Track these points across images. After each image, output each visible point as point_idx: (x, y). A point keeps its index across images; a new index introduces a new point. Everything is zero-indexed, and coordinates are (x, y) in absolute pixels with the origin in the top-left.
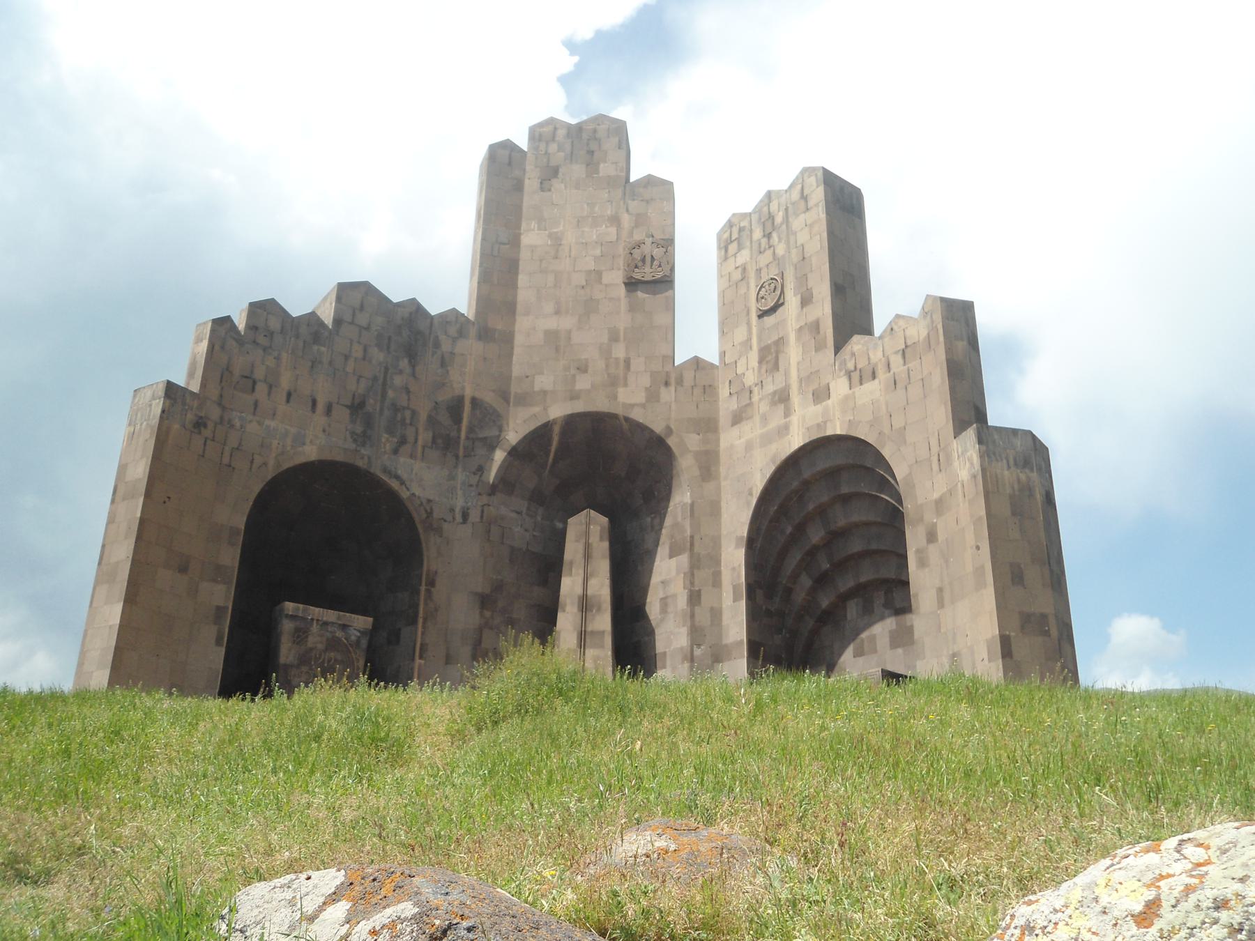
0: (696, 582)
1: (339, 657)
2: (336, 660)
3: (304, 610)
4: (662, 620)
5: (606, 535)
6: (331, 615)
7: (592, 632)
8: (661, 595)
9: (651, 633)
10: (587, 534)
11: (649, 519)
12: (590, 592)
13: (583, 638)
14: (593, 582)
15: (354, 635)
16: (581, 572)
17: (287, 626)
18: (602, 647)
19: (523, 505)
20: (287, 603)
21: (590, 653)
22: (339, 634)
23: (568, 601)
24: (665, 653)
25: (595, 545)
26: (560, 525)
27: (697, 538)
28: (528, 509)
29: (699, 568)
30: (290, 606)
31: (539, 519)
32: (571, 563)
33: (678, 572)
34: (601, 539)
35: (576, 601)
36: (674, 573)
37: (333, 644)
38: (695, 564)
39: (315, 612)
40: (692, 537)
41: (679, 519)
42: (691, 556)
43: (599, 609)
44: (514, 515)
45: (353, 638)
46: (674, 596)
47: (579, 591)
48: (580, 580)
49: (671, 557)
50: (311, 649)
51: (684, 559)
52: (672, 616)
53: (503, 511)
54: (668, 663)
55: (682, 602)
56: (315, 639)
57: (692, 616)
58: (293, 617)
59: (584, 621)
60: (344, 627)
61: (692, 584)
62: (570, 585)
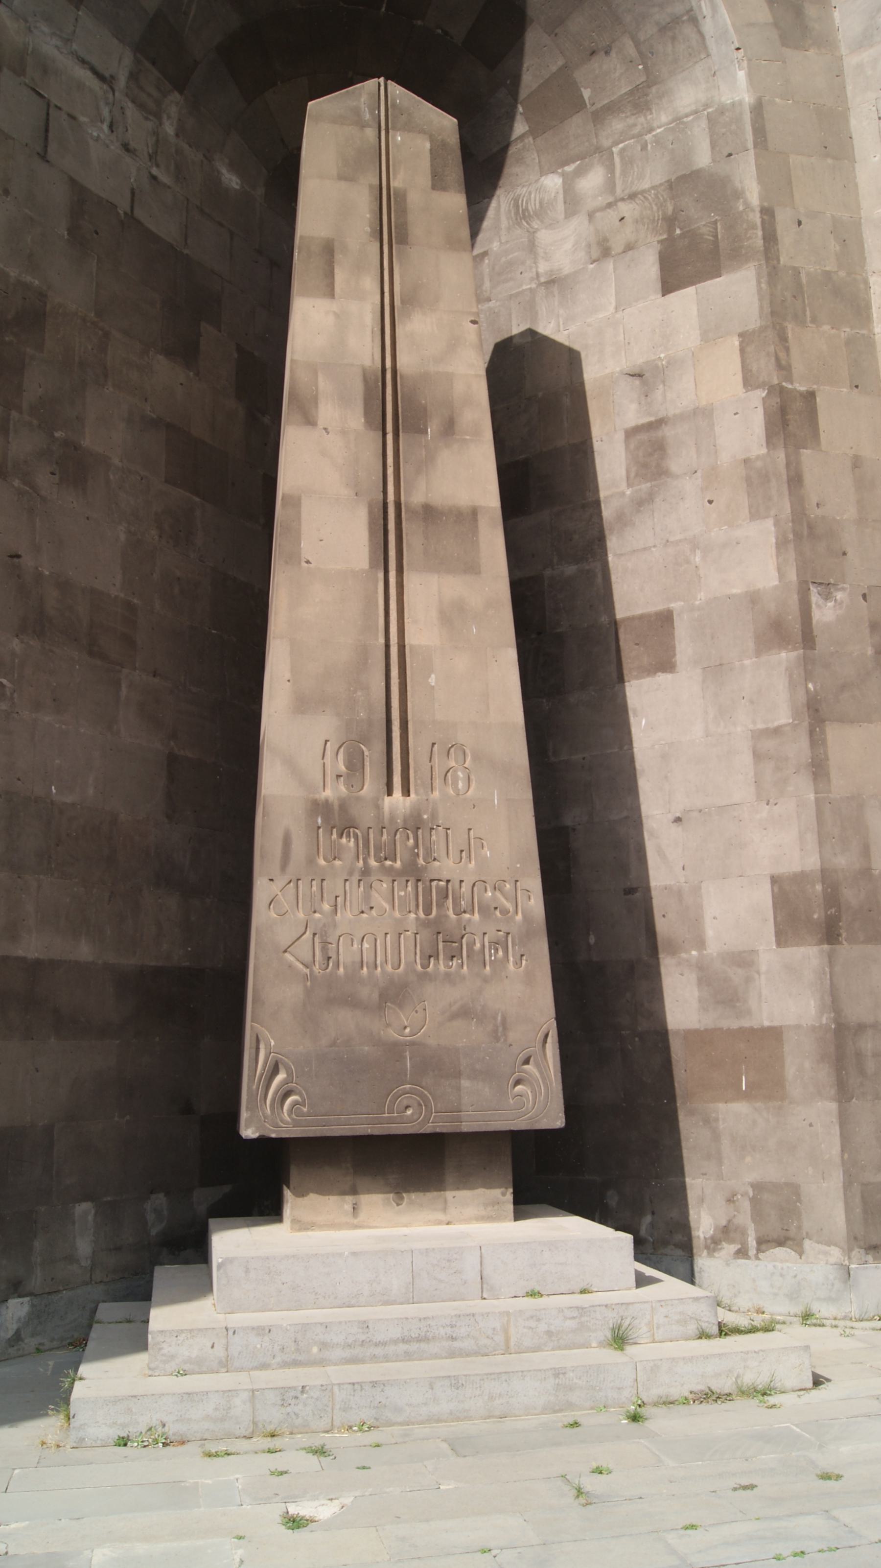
0: (798, 367)
4: (642, 503)
5: (455, 172)
7: (430, 514)
8: (632, 414)
9: (592, 546)
10: (381, 158)
11: (553, 182)
12: (406, 361)
13: (392, 530)
14: (420, 333)
16: (370, 284)
18: (472, 568)
19: (121, 62)
21: (424, 591)
23: (324, 384)
24: (666, 619)
25: (414, 199)
26: (232, 180)
27: (783, 218)
28: (133, 77)
29: (800, 320)
31: (169, 129)
32: (329, 251)
33: (710, 334)
34: (438, 182)
35: (358, 388)
36: (688, 337)
38: (786, 306)
40: (768, 213)
41: (703, 158)
42: (772, 269)
43: (449, 428)
44: (84, 75)
46: (702, 415)
47: (364, 350)
48: (365, 313)
49: (667, 288)
51: (738, 290)
52: (690, 486)
53: (47, 44)
54: (685, 646)
55: (742, 430)
57: (795, 481)
59: (391, 470)
61: (784, 368)
62: (326, 330)
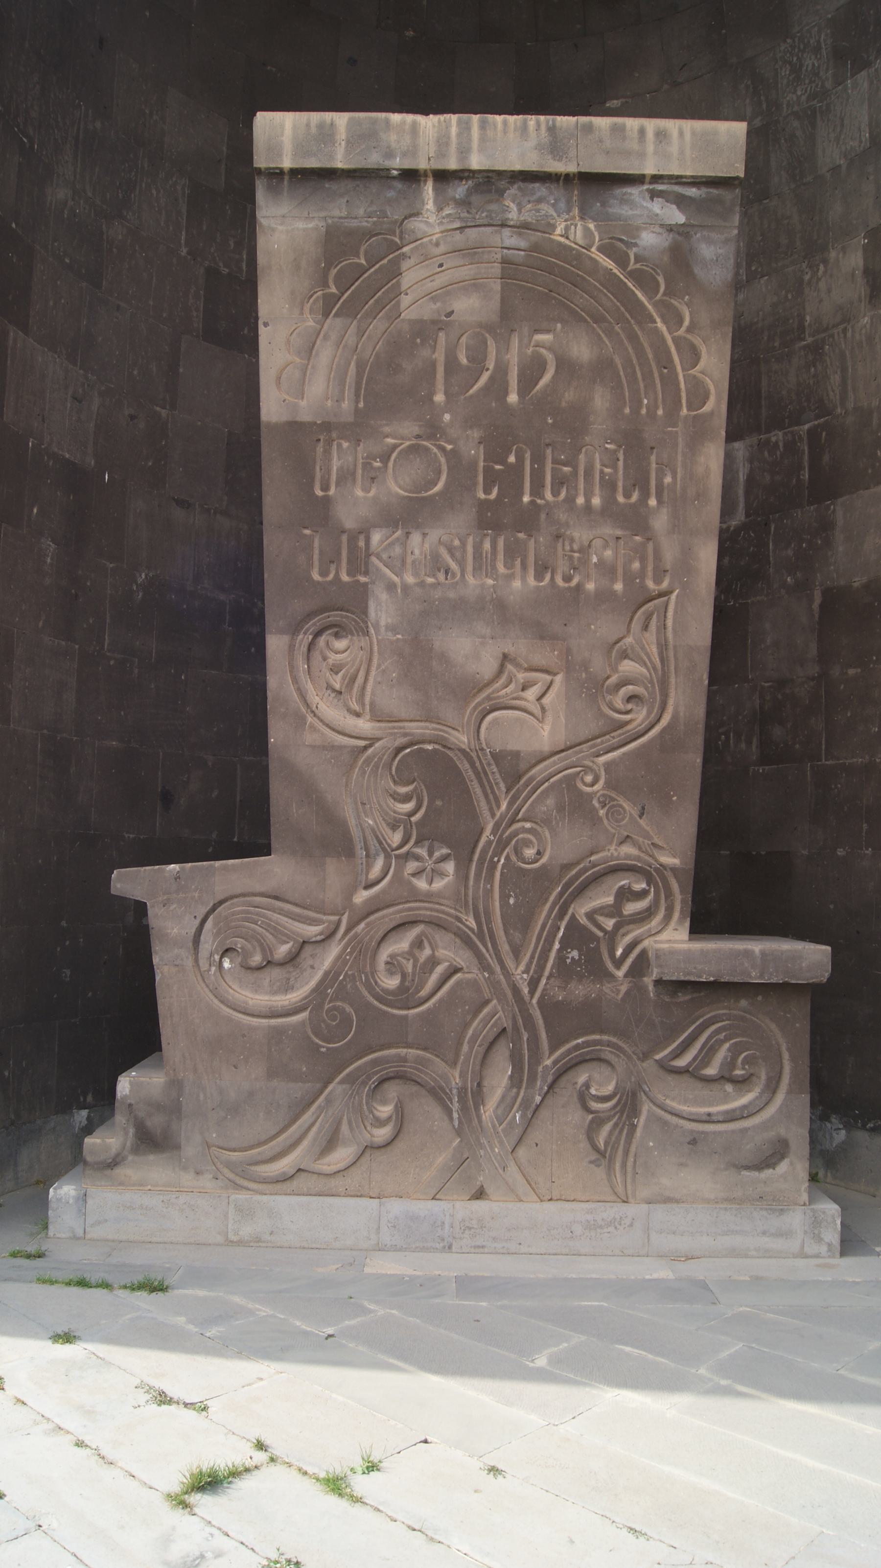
1: (581, 350)
2: (565, 365)
3: (360, 138)
6: (509, 140)
15: (651, 222)
17: (284, 229)
20: (264, 121)
22: (572, 229)
30: (282, 134)
37: (540, 284)
39: (423, 136)
45: (650, 240)
50: (425, 331)
56: (442, 270)
58: (312, 179)
60: (595, 184)
